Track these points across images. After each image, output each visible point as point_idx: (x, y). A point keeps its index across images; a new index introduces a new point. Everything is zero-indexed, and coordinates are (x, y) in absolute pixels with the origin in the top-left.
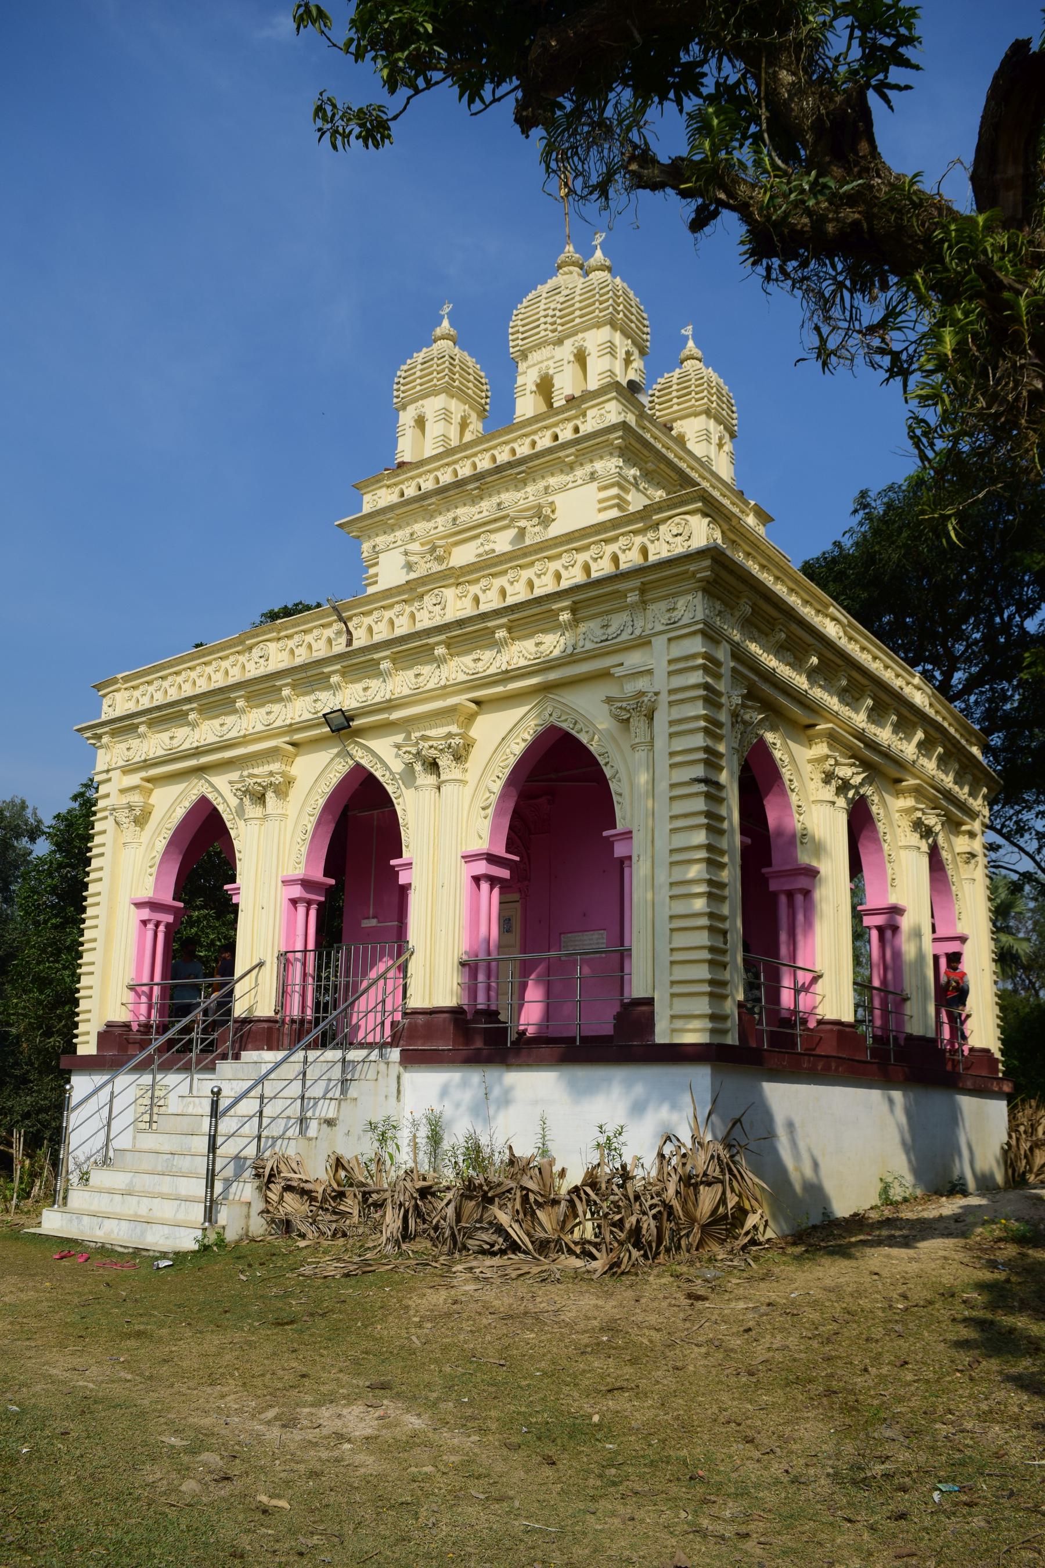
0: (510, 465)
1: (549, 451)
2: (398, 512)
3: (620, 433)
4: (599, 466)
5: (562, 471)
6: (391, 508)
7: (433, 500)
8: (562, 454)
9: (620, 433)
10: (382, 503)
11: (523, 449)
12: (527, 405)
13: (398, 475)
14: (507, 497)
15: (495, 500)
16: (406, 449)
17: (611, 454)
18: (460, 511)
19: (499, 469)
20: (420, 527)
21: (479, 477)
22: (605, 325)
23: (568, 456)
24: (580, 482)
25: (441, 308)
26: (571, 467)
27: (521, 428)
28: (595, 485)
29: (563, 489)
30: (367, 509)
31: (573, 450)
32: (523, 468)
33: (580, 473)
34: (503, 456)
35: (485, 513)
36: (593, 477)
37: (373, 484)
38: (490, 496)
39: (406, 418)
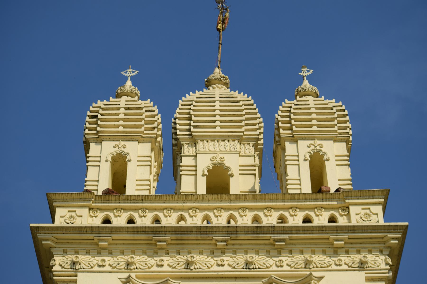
0: (272, 229)
1: (321, 229)
2: (115, 236)
3: (399, 235)
4: (370, 258)
5: (324, 253)
6: (91, 230)
7: (168, 237)
8: (333, 236)
9: (399, 235)
10: (78, 223)
11: (296, 220)
12: (192, 183)
13: (108, 201)
14: (259, 260)
15: (241, 258)
16: (99, 177)
17: (381, 252)
18: (198, 258)
19: (258, 230)
20: (140, 260)
21: (231, 231)
22: (341, 141)
23: (337, 240)
24: (345, 267)
25: (125, 68)
26: (336, 251)
27: (291, 200)
28: (362, 275)
29: (325, 268)
30: (59, 222)
31: (346, 236)
32: (286, 237)
33: (344, 258)
34: (270, 219)
35: (226, 268)
36: (362, 265)
37: (73, 200)
38: (235, 253)
39: (102, 153)
